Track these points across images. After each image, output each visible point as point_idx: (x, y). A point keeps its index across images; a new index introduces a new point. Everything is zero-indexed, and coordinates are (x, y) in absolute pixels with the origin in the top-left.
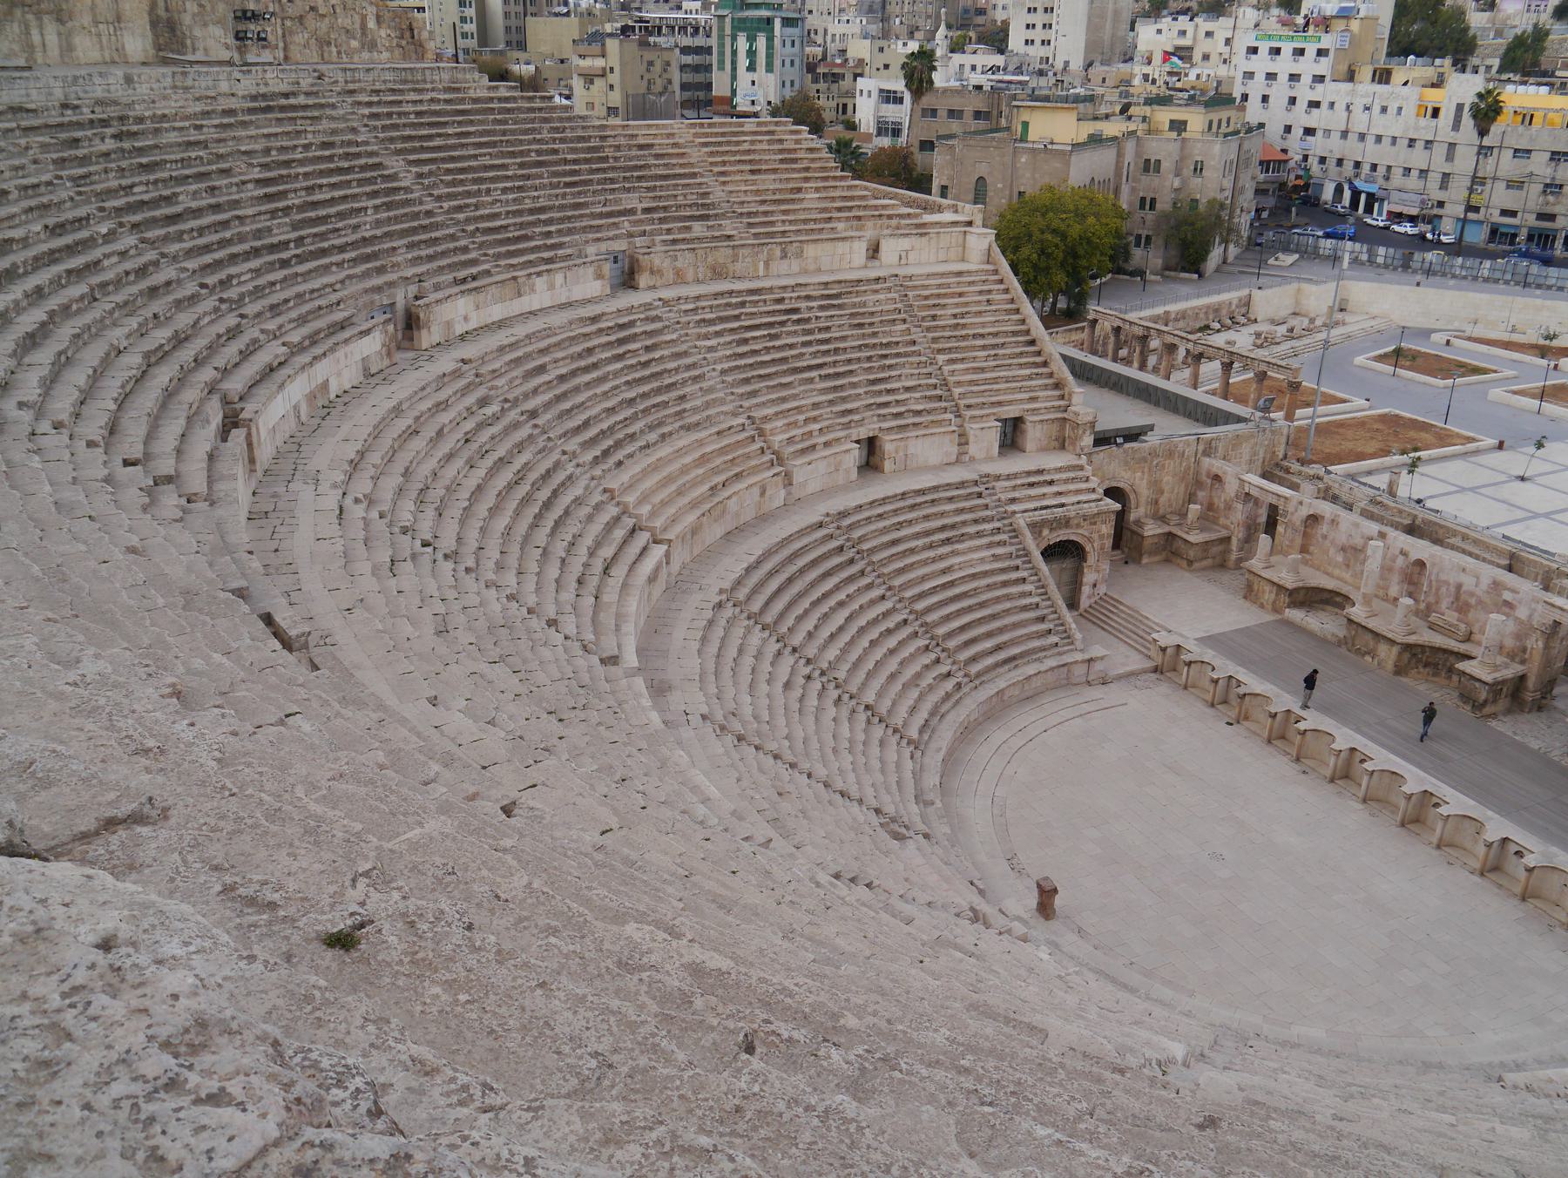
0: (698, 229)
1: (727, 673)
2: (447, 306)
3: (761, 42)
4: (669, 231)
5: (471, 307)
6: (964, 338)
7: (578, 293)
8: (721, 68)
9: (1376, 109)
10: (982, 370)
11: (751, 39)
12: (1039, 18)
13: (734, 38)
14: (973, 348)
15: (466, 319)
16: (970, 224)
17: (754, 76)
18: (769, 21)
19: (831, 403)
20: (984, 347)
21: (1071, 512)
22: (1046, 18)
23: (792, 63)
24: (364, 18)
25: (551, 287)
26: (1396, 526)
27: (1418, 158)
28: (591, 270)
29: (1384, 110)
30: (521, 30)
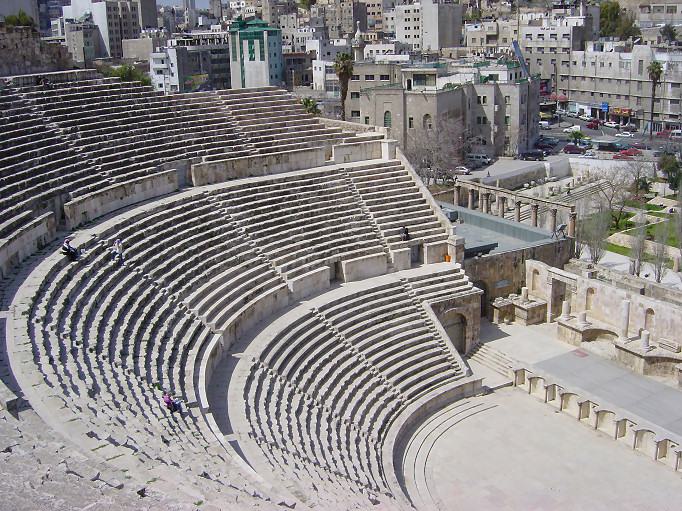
1: (262, 407)
3: (257, 42)
4: (210, 153)
5: (99, 204)
8: (235, 59)
9: (598, 64)
11: (251, 43)
12: (412, 24)
13: (241, 43)
15: (96, 211)
16: (382, 137)
18: (262, 33)
21: (456, 296)
22: (416, 24)
26: (635, 290)
27: (623, 90)
29: (602, 64)
30: (120, 47)
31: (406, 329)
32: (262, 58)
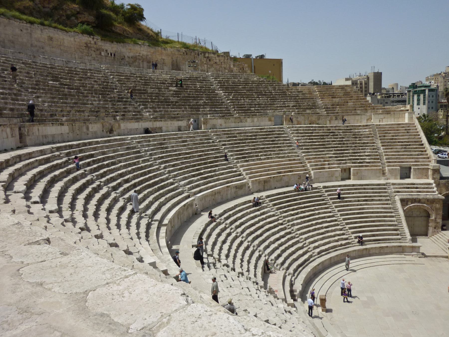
0: (308, 111)
2: (215, 120)
3: (422, 96)
6: (394, 142)
7: (262, 123)
10: (399, 152)
11: (419, 96)
13: (413, 96)
14: (398, 145)
15: (221, 125)
17: (419, 106)
18: (425, 90)
19: (336, 157)
20: (402, 145)
21: (421, 197)
23: (432, 102)
24: (230, 65)
25: (253, 121)
28: (267, 119)
31: (378, 208)
32: (424, 103)
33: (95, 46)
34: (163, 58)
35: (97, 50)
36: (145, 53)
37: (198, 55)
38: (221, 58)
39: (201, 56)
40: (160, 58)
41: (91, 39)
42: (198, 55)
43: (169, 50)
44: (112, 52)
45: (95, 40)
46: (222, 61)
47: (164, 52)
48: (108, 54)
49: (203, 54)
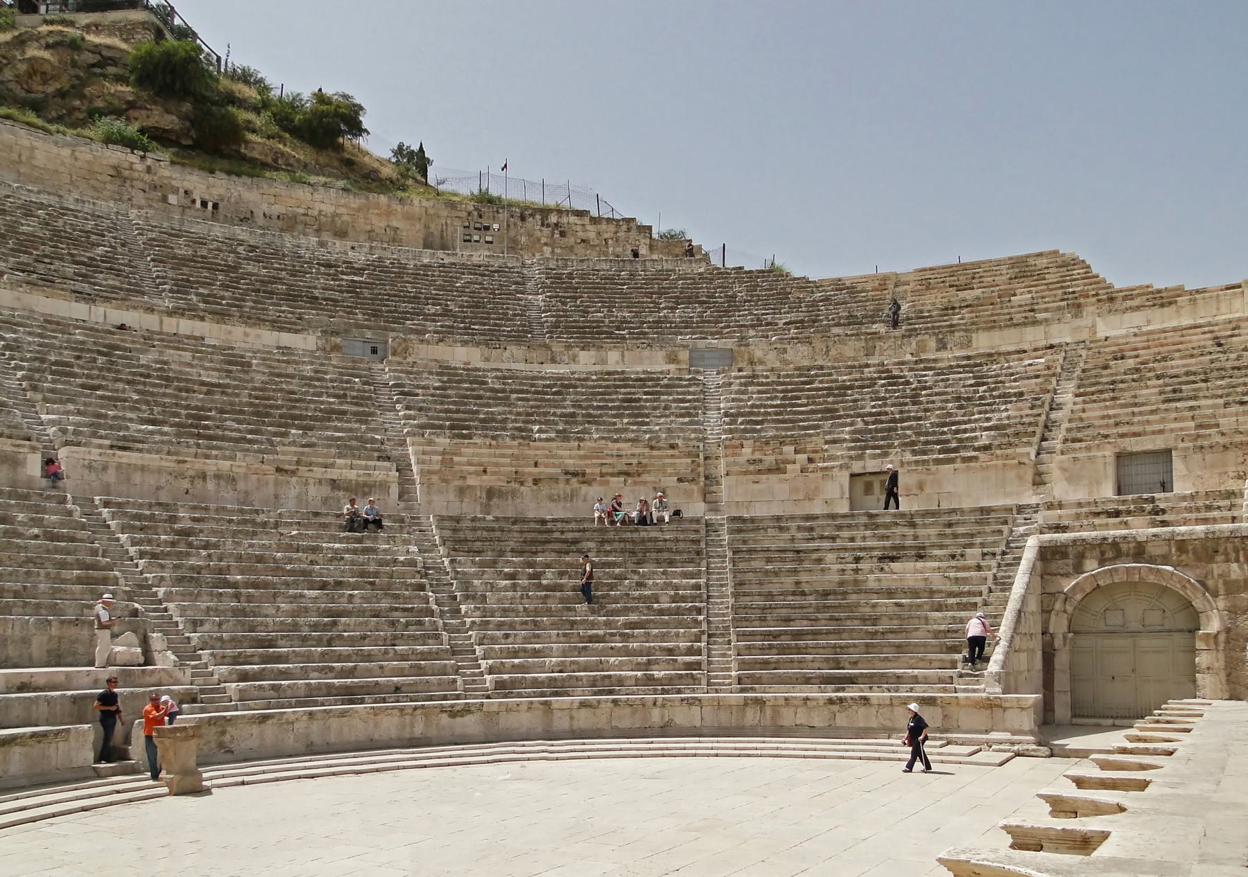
0: (836, 330)
33: (147, 177)
34: (395, 224)
35: (155, 188)
36: (328, 209)
37: (523, 218)
38: (604, 226)
39: (534, 223)
40: (383, 225)
41: (134, 158)
42: (523, 218)
43: (416, 202)
44: (207, 197)
45: (149, 162)
46: (606, 236)
47: (399, 208)
48: (194, 201)
49: (538, 217)
